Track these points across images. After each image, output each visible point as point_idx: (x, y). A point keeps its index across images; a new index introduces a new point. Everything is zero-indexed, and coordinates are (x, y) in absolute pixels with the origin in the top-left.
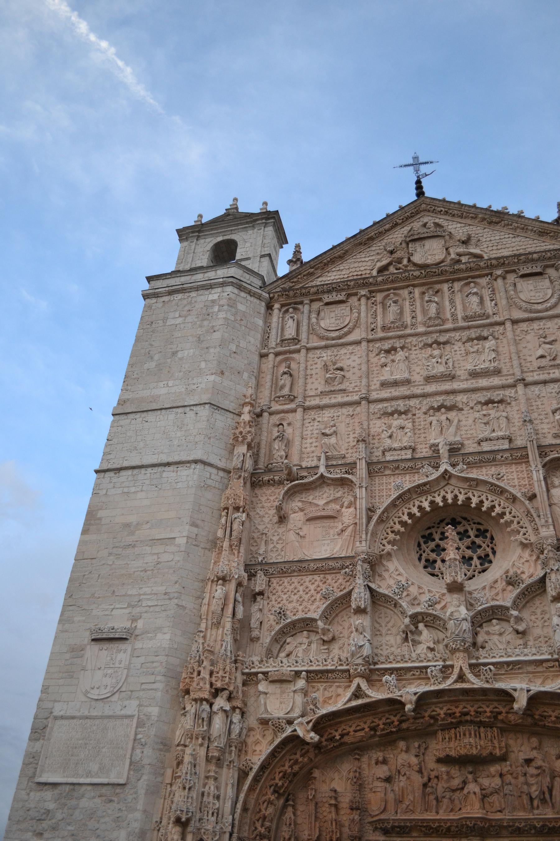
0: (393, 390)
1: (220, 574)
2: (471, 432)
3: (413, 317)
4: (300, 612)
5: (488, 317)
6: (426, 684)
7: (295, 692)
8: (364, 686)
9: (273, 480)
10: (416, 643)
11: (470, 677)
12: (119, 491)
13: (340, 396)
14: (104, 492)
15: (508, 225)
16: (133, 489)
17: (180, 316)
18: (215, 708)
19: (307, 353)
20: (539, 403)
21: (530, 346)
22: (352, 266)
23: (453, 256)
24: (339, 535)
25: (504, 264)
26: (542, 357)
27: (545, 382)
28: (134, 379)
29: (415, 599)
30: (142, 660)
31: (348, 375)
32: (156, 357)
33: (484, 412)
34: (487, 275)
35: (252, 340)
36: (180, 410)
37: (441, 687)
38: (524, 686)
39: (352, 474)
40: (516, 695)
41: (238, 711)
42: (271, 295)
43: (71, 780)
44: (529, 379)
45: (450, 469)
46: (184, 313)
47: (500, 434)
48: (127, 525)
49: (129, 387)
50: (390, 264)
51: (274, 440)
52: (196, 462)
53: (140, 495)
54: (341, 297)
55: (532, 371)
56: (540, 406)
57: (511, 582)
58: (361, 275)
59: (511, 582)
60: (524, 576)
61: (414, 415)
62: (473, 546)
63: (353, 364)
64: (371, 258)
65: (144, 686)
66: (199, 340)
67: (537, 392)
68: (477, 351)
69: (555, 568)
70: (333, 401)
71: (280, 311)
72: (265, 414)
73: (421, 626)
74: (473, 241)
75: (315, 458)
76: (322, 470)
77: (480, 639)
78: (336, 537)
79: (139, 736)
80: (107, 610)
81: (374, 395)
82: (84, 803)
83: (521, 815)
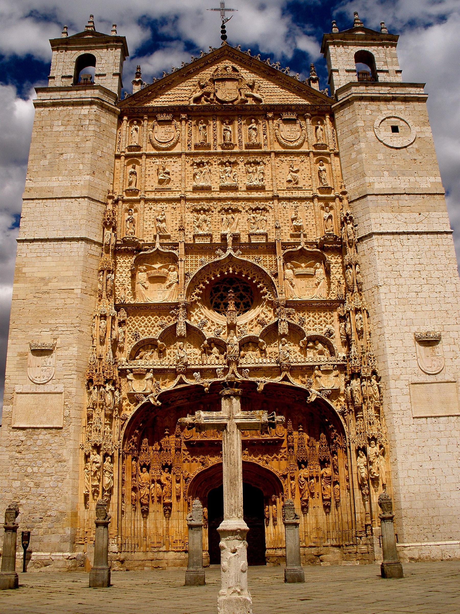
1: (103, 313)
2: (245, 227)
3: (215, 140)
4: (146, 333)
5: (261, 148)
6: (215, 377)
7: (147, 380)
8: (184, 378)
9: (127, 249)
10: (210, 354)
11: (238, 375)
12: (35, 255)
14: (25, 255)
15: (279, 79)
16: (43, 255)
17: (62, 125)
18: (107, 389)
19: (146, 158)
20: (285, 212)
21: (283, 171)
22: (177, 92)
23: (243, 97)
24: (167, 288)
25: (274, 109)
26: (290, 181)
27: (289, 199)
28: (35, 172)
29: (209, 328)
30: (62, 362)
31: (172, 178)
32: (48, 156)
33: (254, 215)
34: (263, 115)
37: (223, 379)
38: (263, 380)
39: (176, 249)
40: (259, 384)
41: (117, 390)
43: (32, 426)
44: (281, 195)
45: (232, 253)
46: (65, 122)
47: (262, 231)
48: (43, 279)
49: (32, 179)
50: (202, 96)
51: (127, 221)
52: (82, 239)
53: (49, 259)
54: (169, 117)
55: (283, 190)
56: (285, 215)
57: (262, 323)
58: (183, 101)
59: (262, 323)
60: (266, 319)
61: (213, 212)
62: (241, 297)
63: (176, 170)
64: (189, 88)
65: (65, 377)
66: (78, 147)
67: (285, 205)
68: (253, 172)
69: (283, 319)
70: (164, 197)
71: (127, 121)
72: (120, 202)
73: (212, 345)
74: (256, 86)
75: (152, 236)
76: (158, 246)
79: (66, 403)
80: (37, 332)
81: (189, 195)
82: (41, 437)
83: (256, 437)
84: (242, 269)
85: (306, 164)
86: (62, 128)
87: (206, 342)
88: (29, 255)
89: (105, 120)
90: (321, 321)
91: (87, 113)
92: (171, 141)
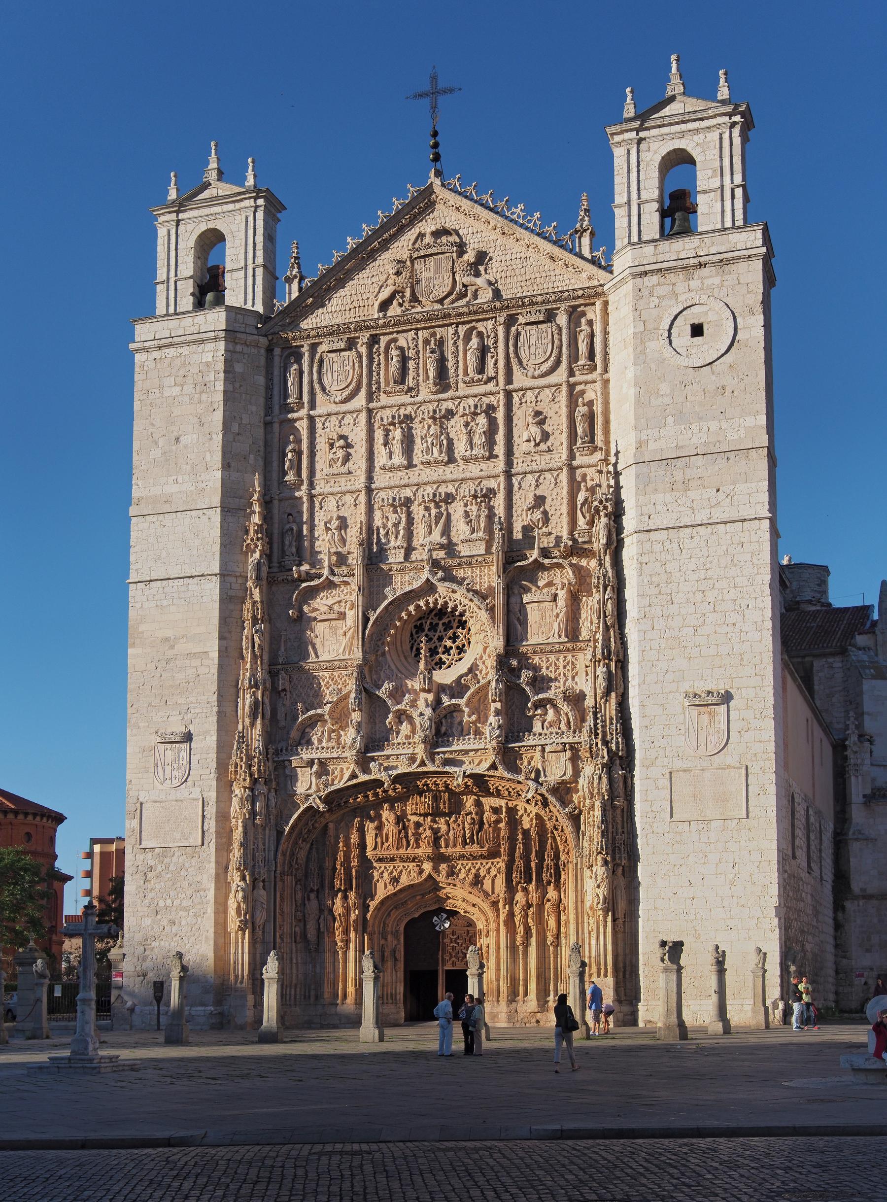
0: (391, 475)
9: (287, 579)
13: (343, 480)
16: (165, 603)
26: (529, 441)
32: (161, 442)
34: (492, 318)
35: (254, 409)
36: (194, 513)
37: (408, 771)
39: (353, 575)
42: (270, 338)
45: (430, 578)
48: (167, 639)
72: (276, 502)
77: (443, 729)
78: (341, 637)
84: (447, 598)
85: (557, 405)
86: (176, 391)
87: (390, 716)
88: (146, 605)
89: (240, 365)
90: (559, 675)
91: (211, 359)
92: (347, 386)
